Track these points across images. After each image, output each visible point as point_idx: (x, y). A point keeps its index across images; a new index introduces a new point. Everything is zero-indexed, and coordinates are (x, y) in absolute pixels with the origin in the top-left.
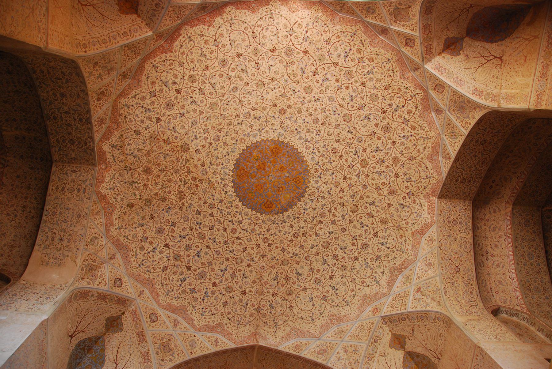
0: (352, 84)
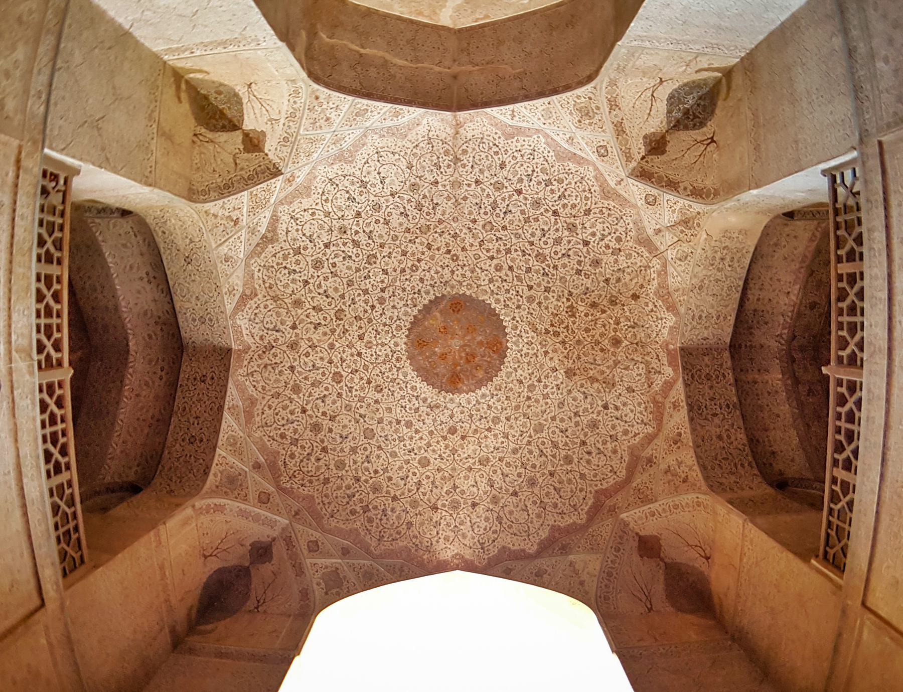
0: (371, 478)
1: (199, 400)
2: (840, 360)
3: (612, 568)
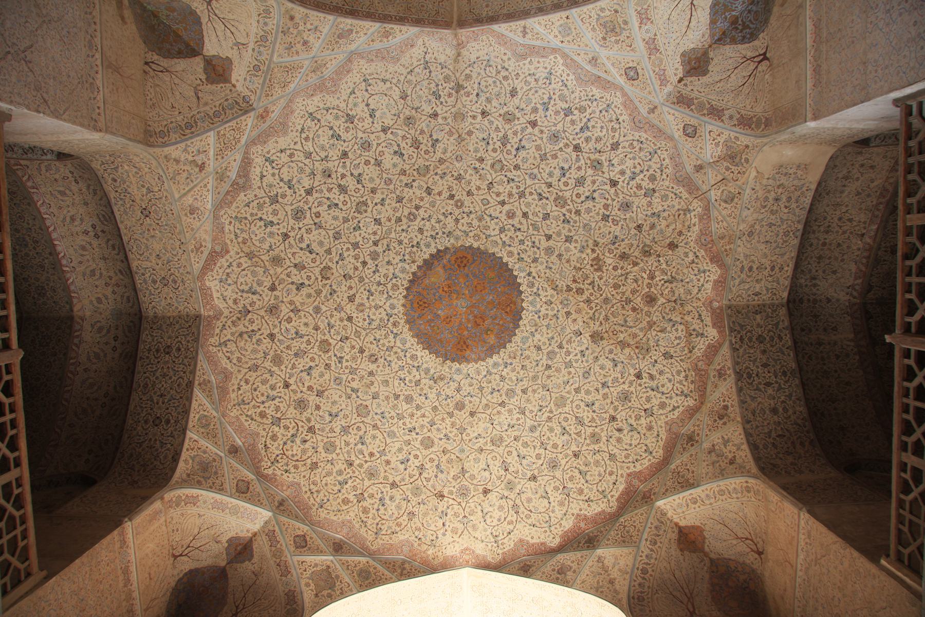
0: (366, 462)
1: (164, 375)
2: (907, 329)
3: (647, 564)
